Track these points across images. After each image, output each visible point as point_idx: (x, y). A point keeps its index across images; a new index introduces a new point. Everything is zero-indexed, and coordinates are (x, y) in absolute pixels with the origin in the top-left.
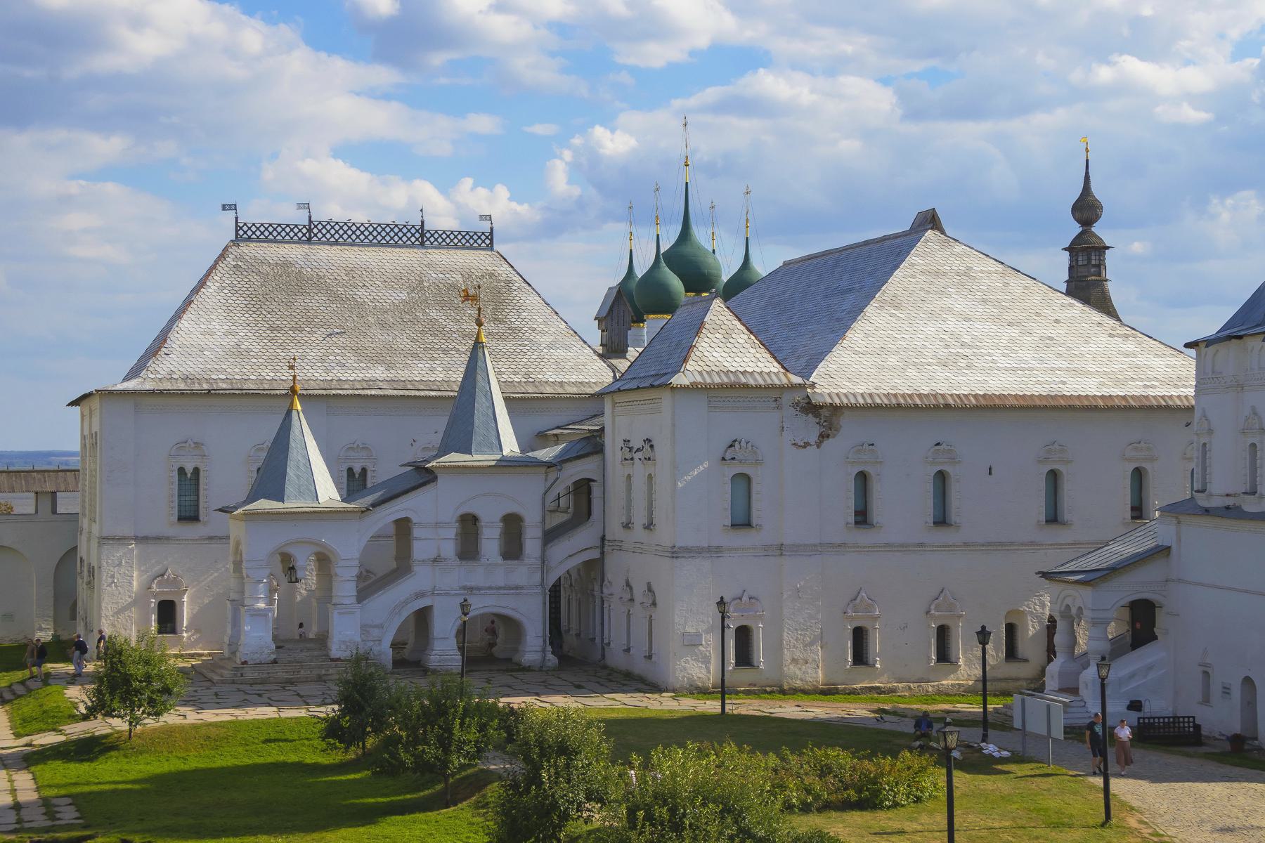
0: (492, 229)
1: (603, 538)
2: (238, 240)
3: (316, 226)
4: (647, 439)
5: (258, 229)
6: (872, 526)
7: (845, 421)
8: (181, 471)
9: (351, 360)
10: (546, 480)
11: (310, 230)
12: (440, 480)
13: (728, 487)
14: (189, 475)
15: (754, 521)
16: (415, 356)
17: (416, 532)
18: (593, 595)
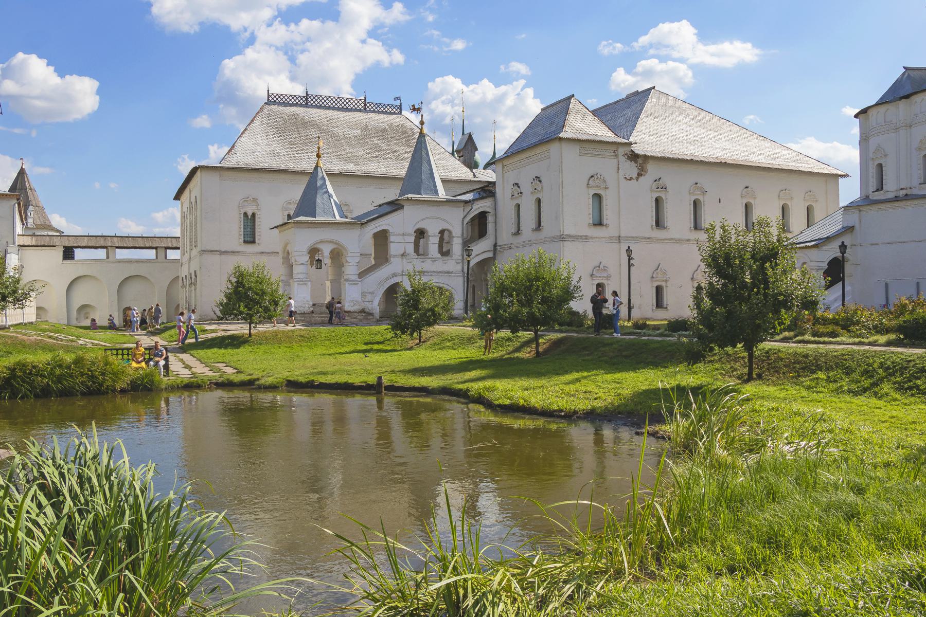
0: (401, 104)
1: (495, 245)
2: (269, 103)
3: (310, 97)
4: (536, 177)
5: (279, 97)
6: (664, 228)
7: (651, 167)
8: (245, 214)
9: (335, 161)
10: (464, 211)
11: (307, 99)
12: (405, 207)
13: (591, 201)
14: (250, 217)
15: (605, 222)
16: (370, 160)
17: (392, 238)
18: (487, 280)
